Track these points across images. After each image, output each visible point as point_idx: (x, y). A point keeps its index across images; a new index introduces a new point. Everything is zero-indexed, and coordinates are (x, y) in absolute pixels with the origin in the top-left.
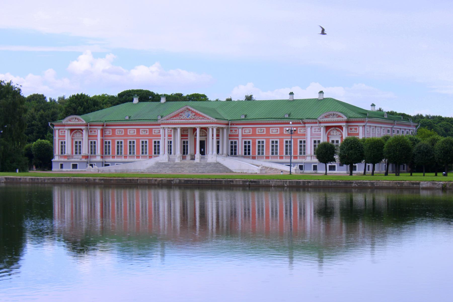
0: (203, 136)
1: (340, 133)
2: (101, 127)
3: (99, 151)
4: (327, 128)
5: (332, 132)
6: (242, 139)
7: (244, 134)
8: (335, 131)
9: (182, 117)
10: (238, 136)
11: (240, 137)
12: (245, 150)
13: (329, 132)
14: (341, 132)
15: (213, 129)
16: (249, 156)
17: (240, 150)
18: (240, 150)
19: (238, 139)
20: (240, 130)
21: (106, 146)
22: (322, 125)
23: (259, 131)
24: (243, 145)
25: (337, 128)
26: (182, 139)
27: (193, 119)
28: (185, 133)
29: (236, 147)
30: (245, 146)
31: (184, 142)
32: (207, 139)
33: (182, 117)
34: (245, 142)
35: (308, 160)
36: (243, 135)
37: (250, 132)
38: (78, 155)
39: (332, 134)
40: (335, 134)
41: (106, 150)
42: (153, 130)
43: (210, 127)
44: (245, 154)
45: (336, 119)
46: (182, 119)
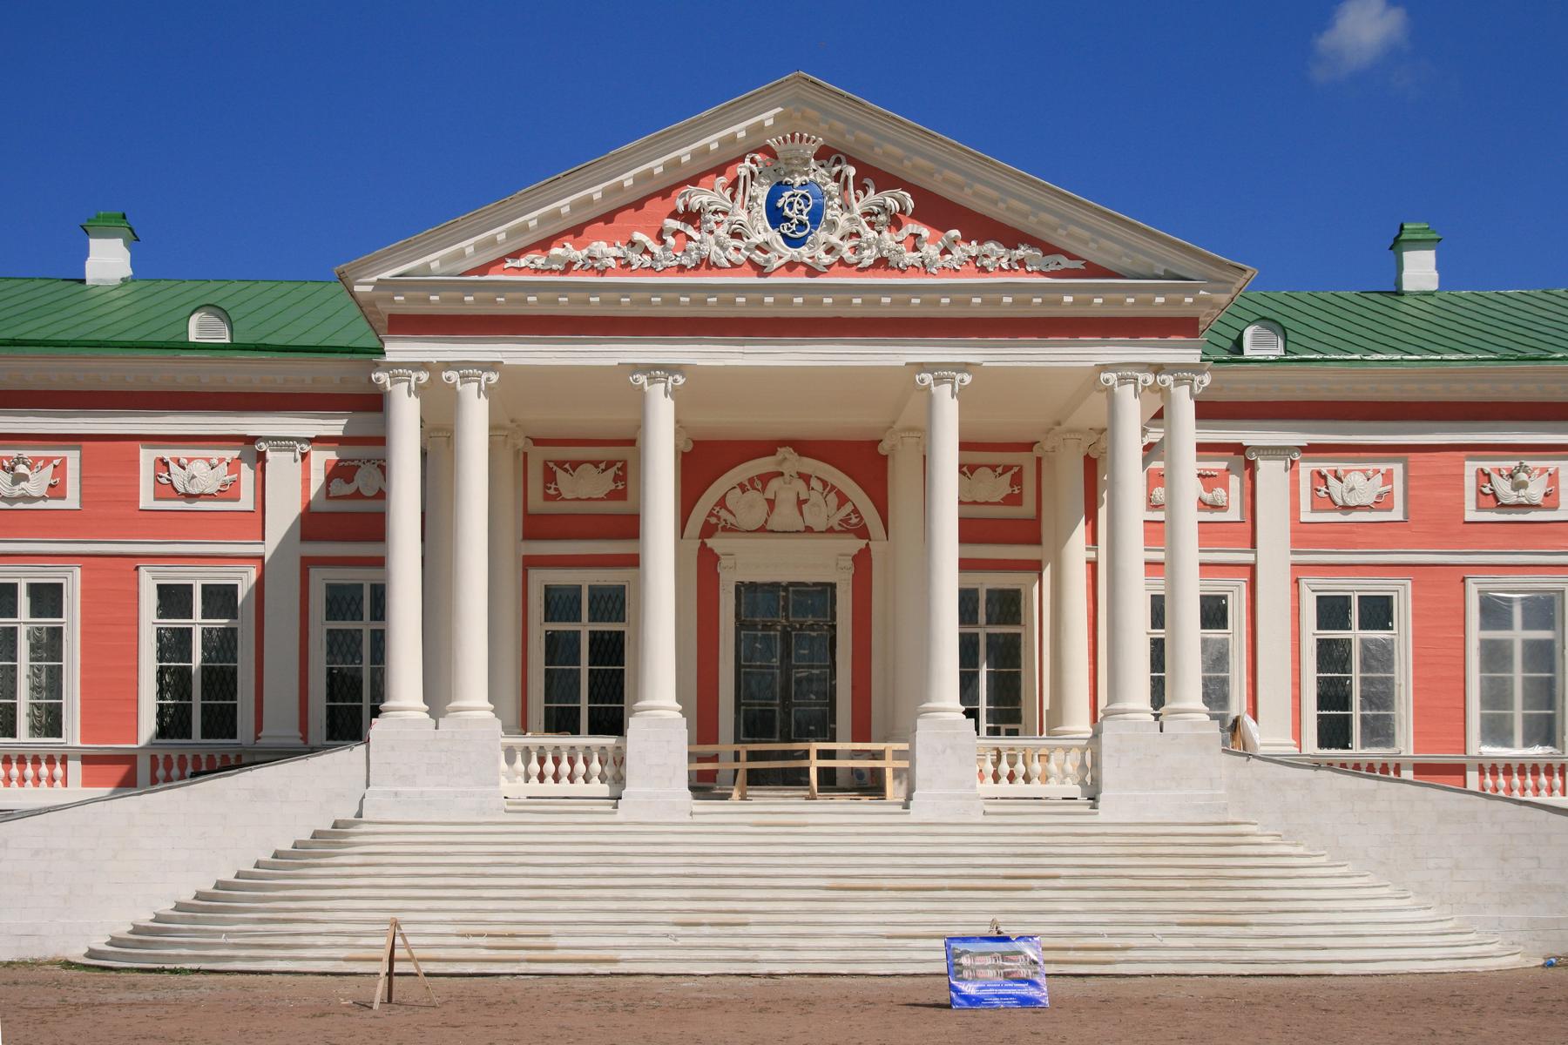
0: (809, 530)
9: (707, 243)
11: (1274, 553)
16: (1376, 753)
20: (1270, 473)
23: (1504, 488)
24: (1311, 633)
26: (530, 562)
28: (585, 489)
31: (560, 604)
32: (862, 562)
33: (707, 243)
34: (1332, 611)
36: (1302, 536)
37: (1383, 502)
42: (147, 457)
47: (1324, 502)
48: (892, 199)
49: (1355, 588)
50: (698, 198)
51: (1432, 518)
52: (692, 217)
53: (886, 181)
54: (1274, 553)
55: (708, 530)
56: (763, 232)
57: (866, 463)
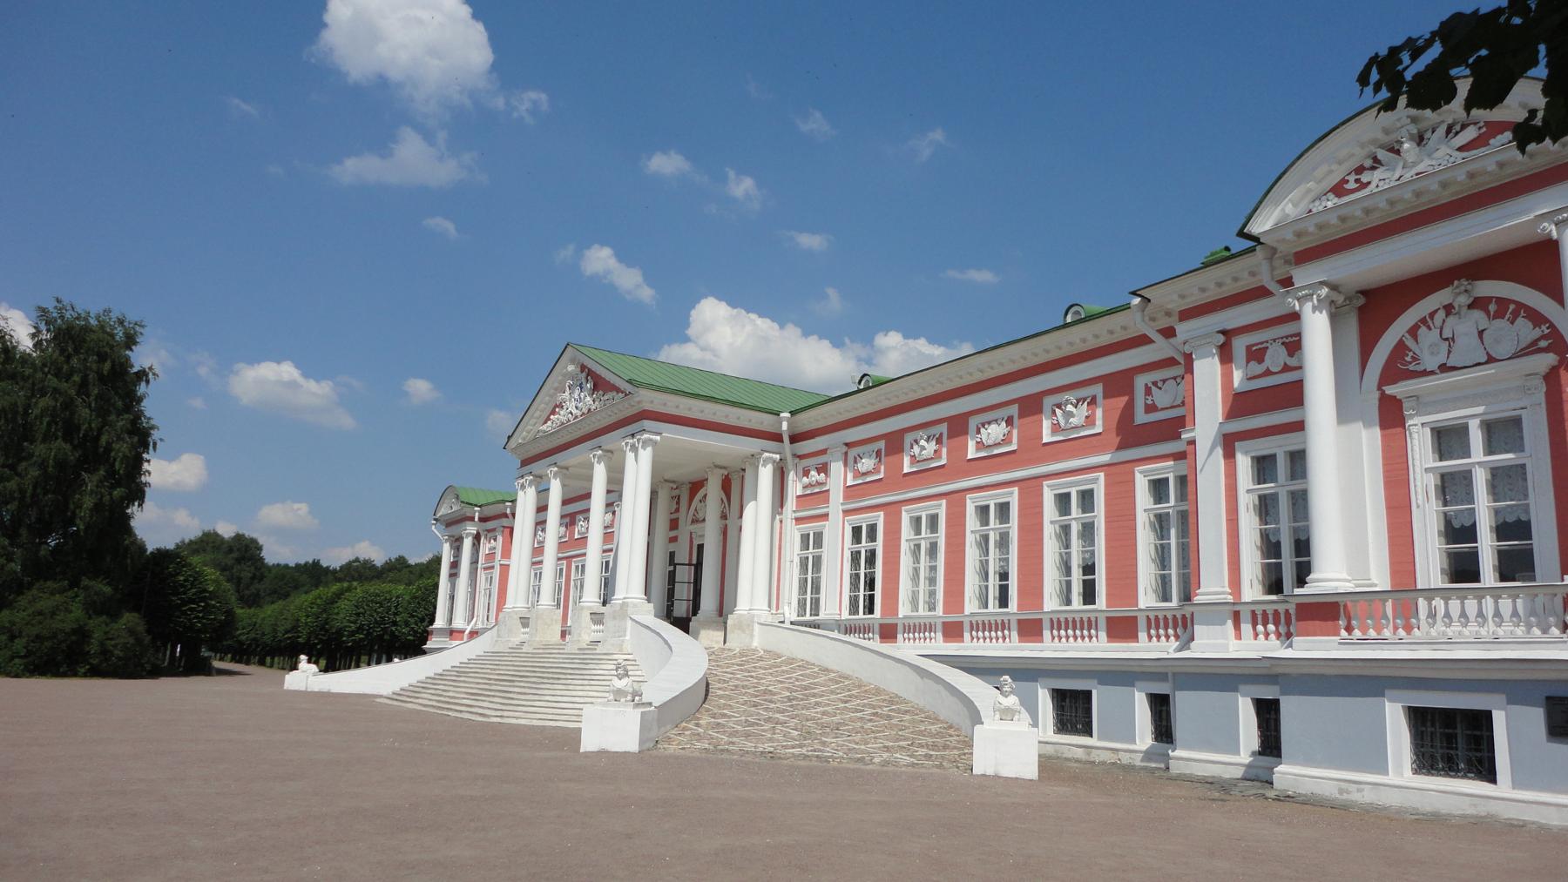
1: (1525, 331)
5: (1428, 337)
6: (847, 512)
8: (1466, 326)
13: (1401, 348)
14: (1536, 318)
25: (1487, 288)
35: (1216, 643)
36: (850, 492)
39: (1430, 363)
40: (1468, 348)
47: (858, 474)
49: (863, 520)
55: (693, 522)
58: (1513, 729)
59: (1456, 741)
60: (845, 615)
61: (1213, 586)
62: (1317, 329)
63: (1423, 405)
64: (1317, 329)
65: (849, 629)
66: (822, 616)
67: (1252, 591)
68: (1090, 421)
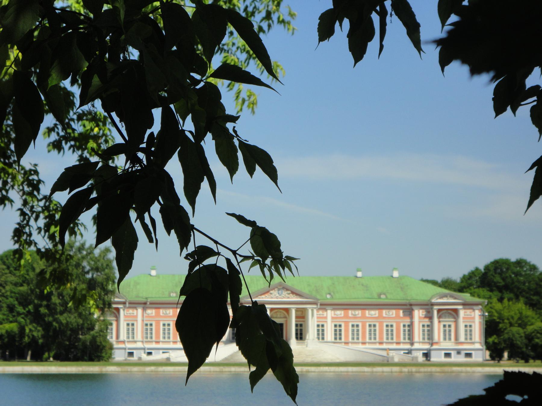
0: (281, 318)
2: (143, 305)
3: (139, 335)
4: (439, 311)
7: (333, 316)
10: (326, 318)
11: (329, 320)
12: (336, 334)
15: (312, 310)
17: (329, 335)
18: (329, 335)
19: (326, 322)
21: (147, 329)
22: (436, 307)
24: (333, 328)
25: (450, 311)
27: (288, 298)
29: (323, 330)
30: (336, 330)
32: (286, 321)
34: (335, 326)
35: (416, 346)
36: (332, 318)
38: (447, 340)
41: (147, 333)
43: (310, 308)
44: (336, 339)
45: (452, 301)
46: (272, 298)
47: (335, 314)
48: (289, 292)
49: (338, 324)
50: (271, 292)
51: (346, 316)
52: (271, 294)
53: (287, 290)
54: (329, 320)
56: (277, 295)
57: (287, 310)
58: (453, 353)
59: (448, 355)
60: (333, 340)
61: (416, 339)
62: (435, 313)
63: (443, 321)
64: (435, 313)
65: (334, 343)
66: (325, 340)
67: (421, 340)
68: (392, 314)
